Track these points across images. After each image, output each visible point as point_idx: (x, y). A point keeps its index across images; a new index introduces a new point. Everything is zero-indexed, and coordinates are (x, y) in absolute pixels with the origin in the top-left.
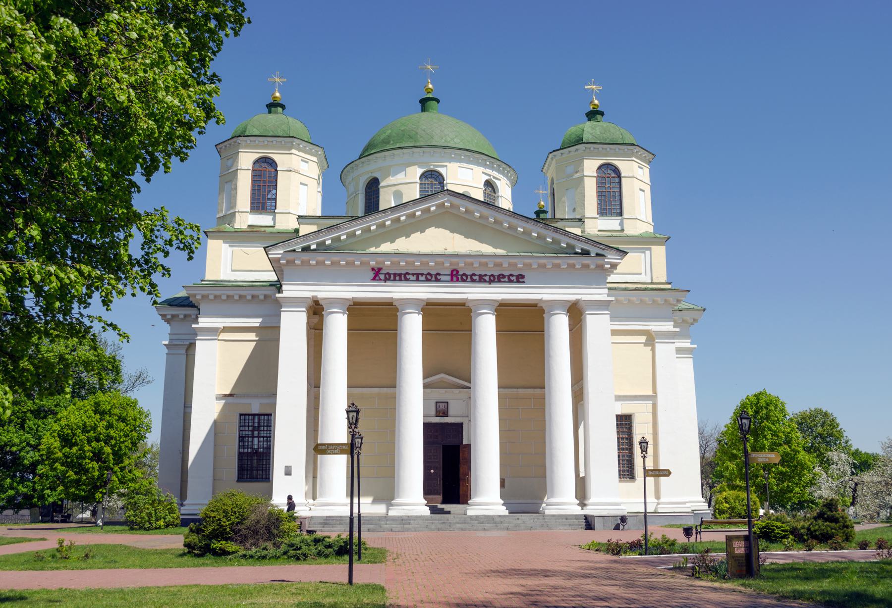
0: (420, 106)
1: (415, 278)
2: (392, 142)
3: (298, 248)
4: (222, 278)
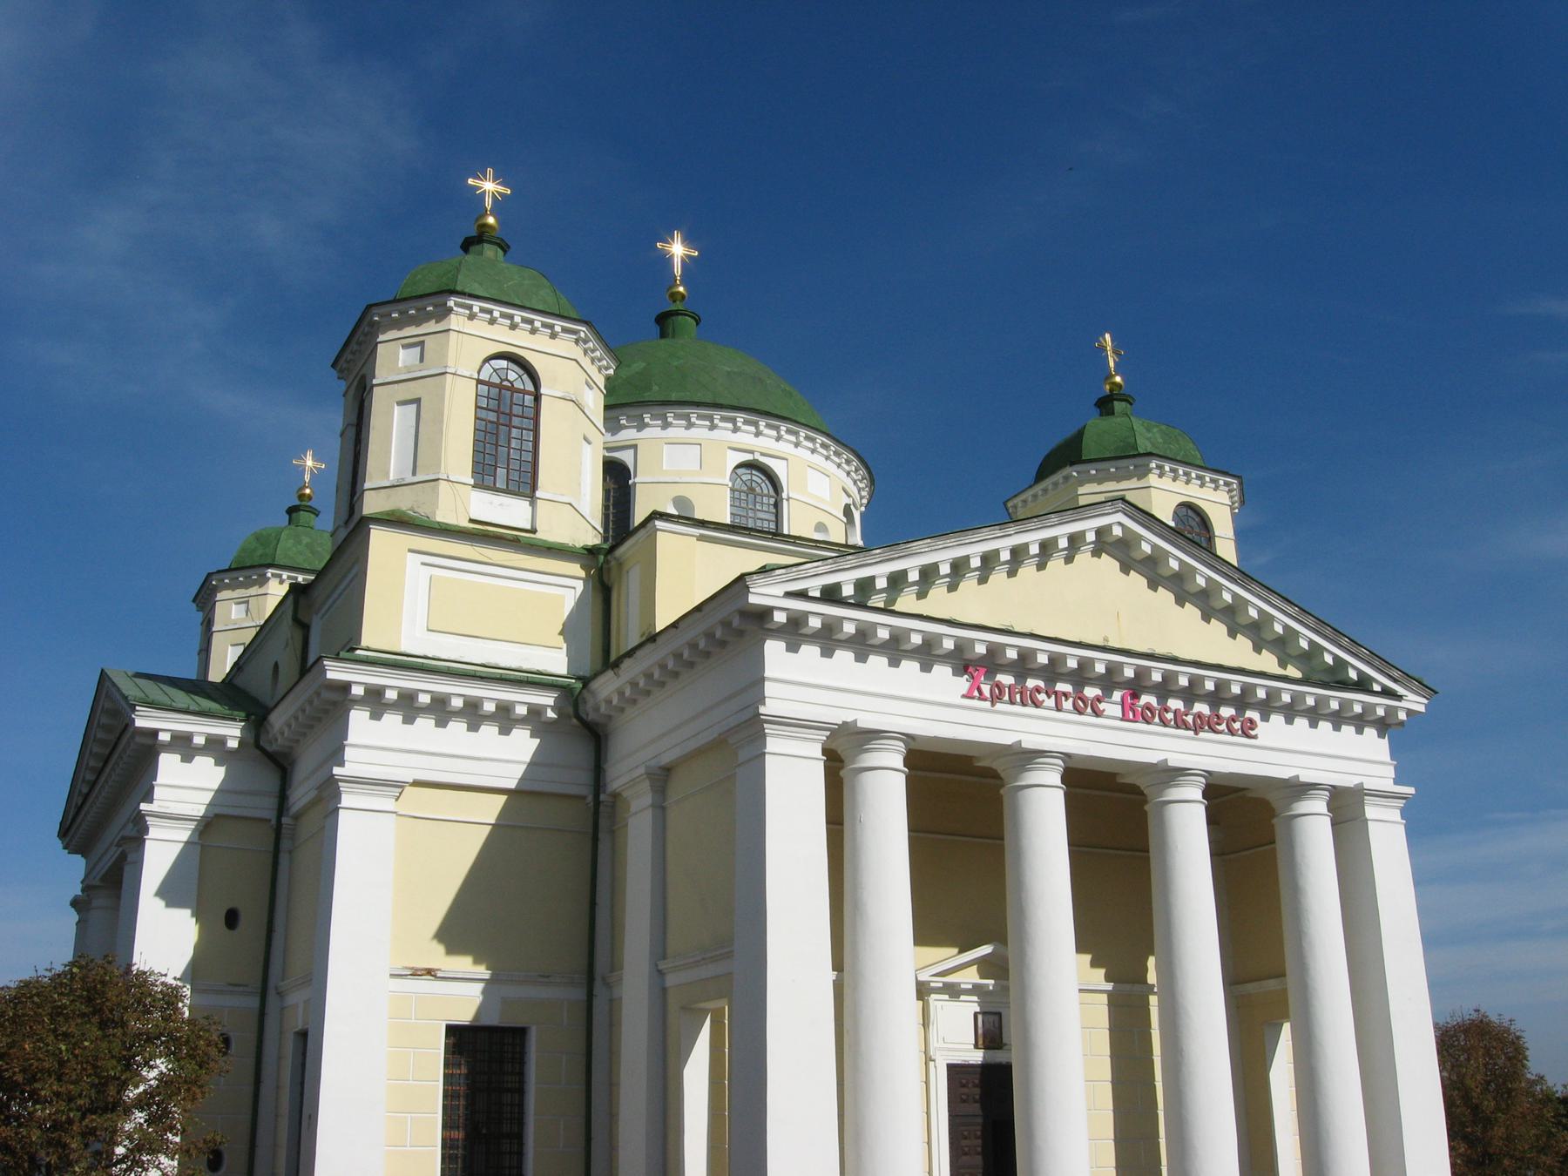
0: (656, 329)
1: (1051, 702)
2: (656, 388)
3: (814, 588)
4: (403, 649)
